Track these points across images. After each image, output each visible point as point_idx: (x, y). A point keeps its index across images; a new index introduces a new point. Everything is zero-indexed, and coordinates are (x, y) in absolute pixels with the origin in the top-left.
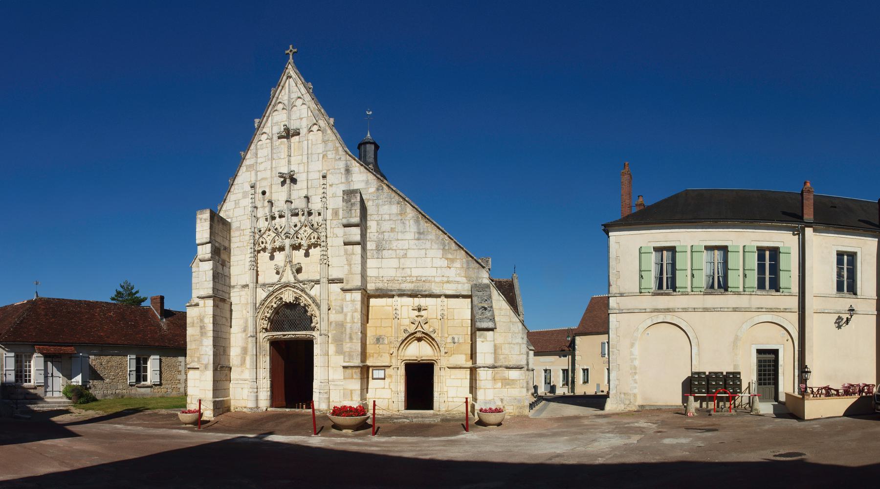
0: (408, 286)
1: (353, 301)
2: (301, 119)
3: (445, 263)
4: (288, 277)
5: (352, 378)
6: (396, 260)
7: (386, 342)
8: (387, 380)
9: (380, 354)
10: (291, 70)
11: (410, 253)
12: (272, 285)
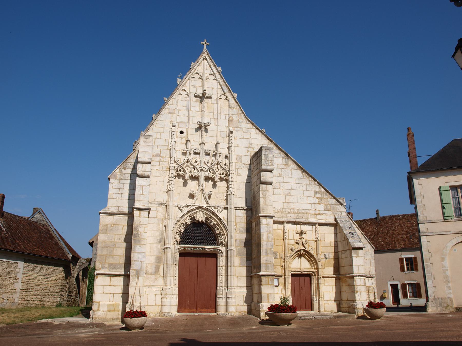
0: (292, 217)
2: (213, 88)
3: (317, 201)
5: (268, 284)
6: (284, 197)
7: (278, 257)
8: (281, 287)
10: (205, 54)
11: (293, 193)
12: (187, 206)
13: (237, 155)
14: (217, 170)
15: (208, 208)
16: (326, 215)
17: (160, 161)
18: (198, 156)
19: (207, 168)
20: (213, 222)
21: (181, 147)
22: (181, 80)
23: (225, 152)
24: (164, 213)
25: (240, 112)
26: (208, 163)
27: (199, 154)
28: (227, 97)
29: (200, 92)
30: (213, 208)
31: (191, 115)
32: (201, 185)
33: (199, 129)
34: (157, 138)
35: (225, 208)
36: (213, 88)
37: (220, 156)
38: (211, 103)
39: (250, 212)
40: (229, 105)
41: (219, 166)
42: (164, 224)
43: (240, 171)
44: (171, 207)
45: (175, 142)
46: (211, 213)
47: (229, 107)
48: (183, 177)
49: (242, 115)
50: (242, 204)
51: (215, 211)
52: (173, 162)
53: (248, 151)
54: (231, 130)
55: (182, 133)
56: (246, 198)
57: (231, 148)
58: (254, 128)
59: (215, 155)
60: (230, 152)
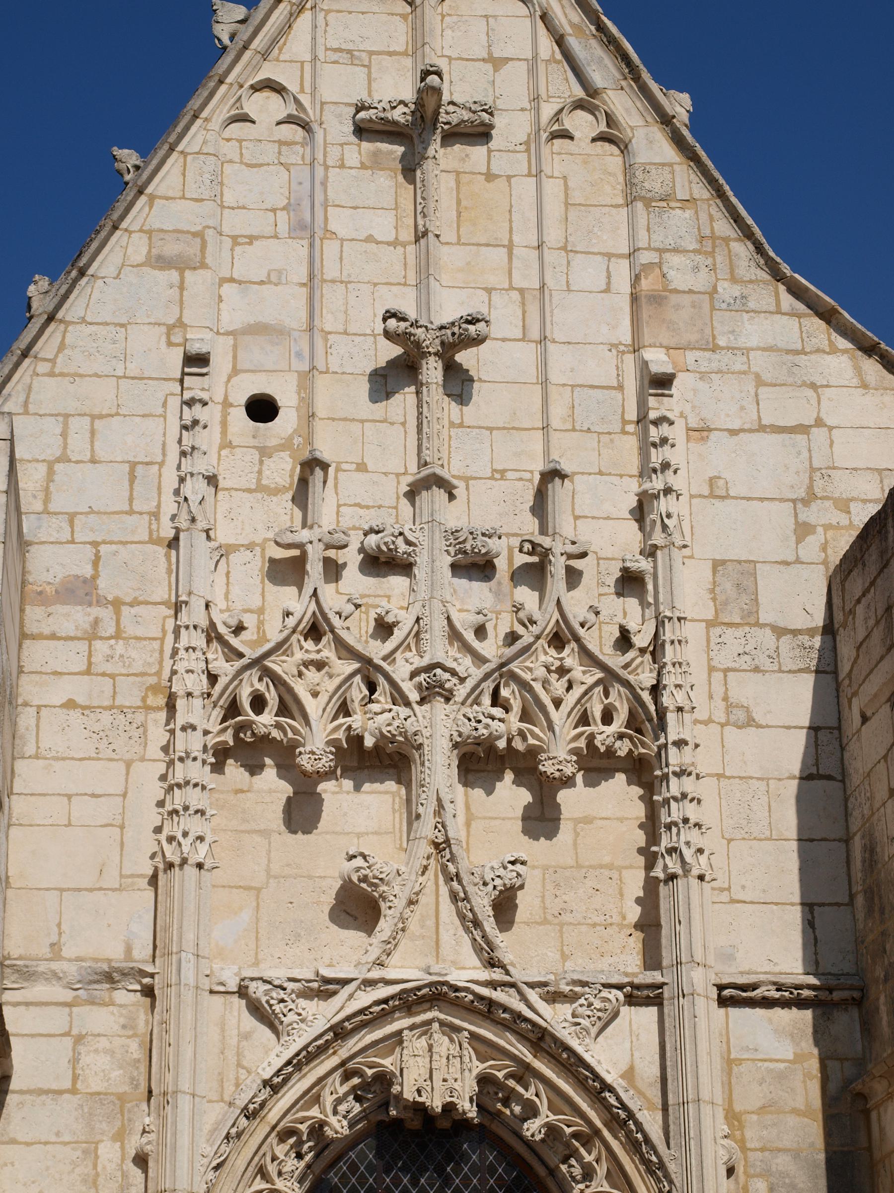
2: (498, 63)
4: (431, 948)
12: (325, 988)
13: (717, 565)
14: (558, 686)
15: (498, 995)
17: (92, 635)
18: (397, 583)
19: (477, 673)
20: (546, 1116)
21: (255, 518)
22: (240, 12)
23: (614, 541)
24: (135, 1050)
25: (724, 227)
26: (480, 631)
27: (405, 567)
28: (610, 120)
29: (395, 89)
30: (533, 996)
31: (331, 270)
32: (427, 811)
33: (396, 375)
34: (64, 459)
35: (641, 995)
36: (498, 63)
37: (573, 577)
38: (490, 177)
39: (846, 1022)
40: (630, 183)
41: (570, 657)
42: (134, 1142)
43: (745, 689)
44: (188, 996)
45: (212, 480)
46: (522, 1036)
47: (632, 194)
48: (285, 755)
49: (743, 250)
50: (778, 951)
51: (556, 1018)
52: (199, 640)
53: (803, 530)
54: (655, 369)
55: (262, 409)
56: (809, 907)
57: (664, 505)
58: (843, 343)
59: (535, 573)
60: (658, 538)
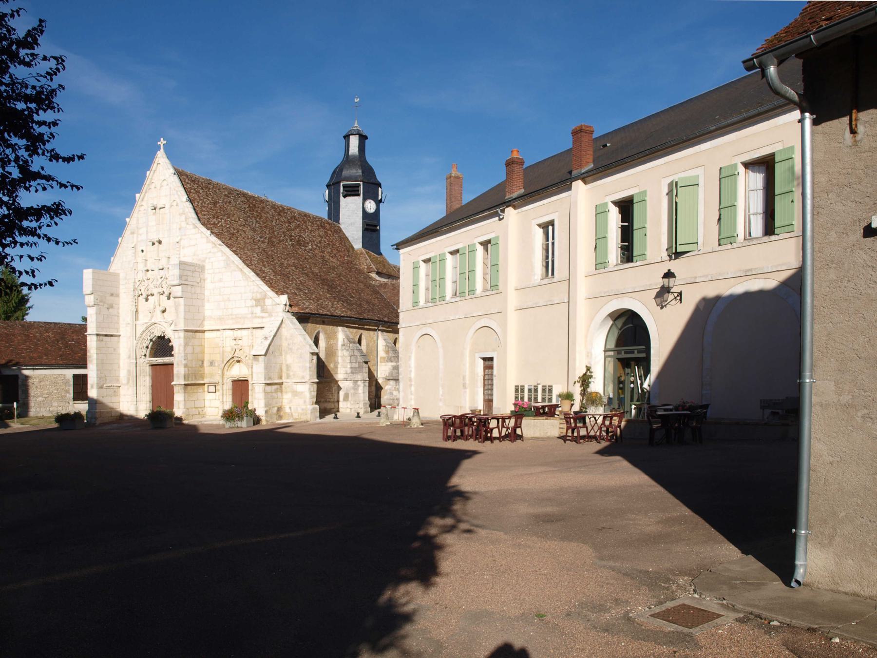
1: (179, 338)
9: (212, 375)
16: (263, 317)
21: (141, 267)
